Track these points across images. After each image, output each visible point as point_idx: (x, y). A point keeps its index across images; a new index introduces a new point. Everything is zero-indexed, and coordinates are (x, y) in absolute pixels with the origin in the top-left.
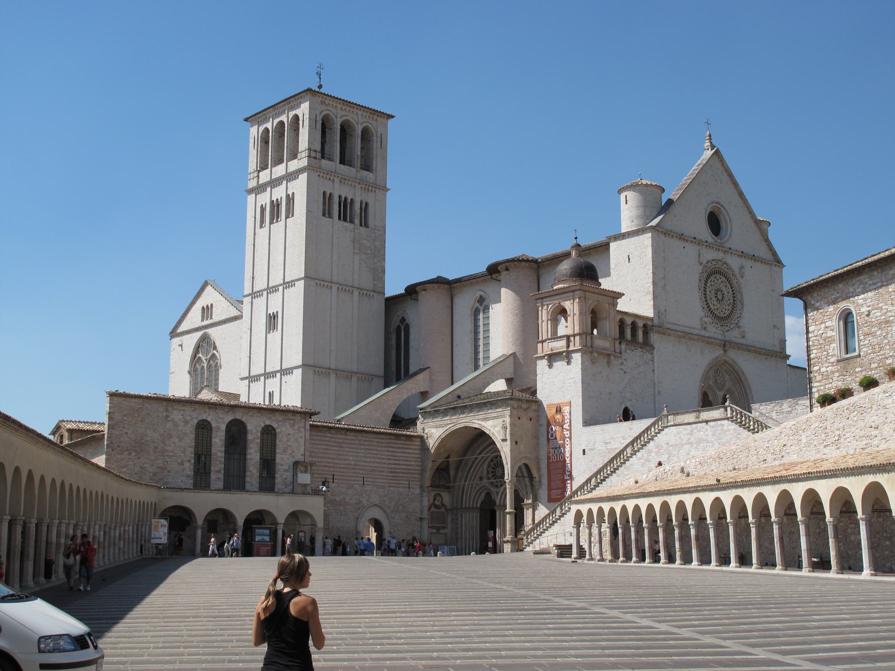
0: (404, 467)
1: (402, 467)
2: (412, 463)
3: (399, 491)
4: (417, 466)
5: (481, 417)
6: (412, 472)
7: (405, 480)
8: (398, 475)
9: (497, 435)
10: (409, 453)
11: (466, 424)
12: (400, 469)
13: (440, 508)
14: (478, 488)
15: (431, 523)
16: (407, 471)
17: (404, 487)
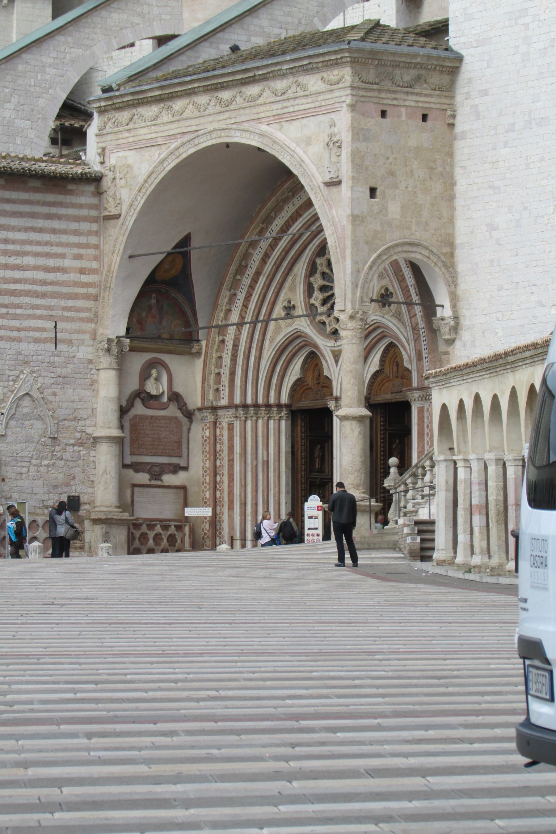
0: (40, 275)
1: (29, 274)
2: (68, 263)
3: (20, 353)
4: (82, 271)
5: (265, 111)
6: (65, 290)
7: (41, 317)
8: (16, 300)
9: (313, 168)
10: (54, 231)
12: (25, 281)
13: (164, 407)
14: (280, 338)
15: (132, 454)
16: (49, 288)
17: (37, 341)
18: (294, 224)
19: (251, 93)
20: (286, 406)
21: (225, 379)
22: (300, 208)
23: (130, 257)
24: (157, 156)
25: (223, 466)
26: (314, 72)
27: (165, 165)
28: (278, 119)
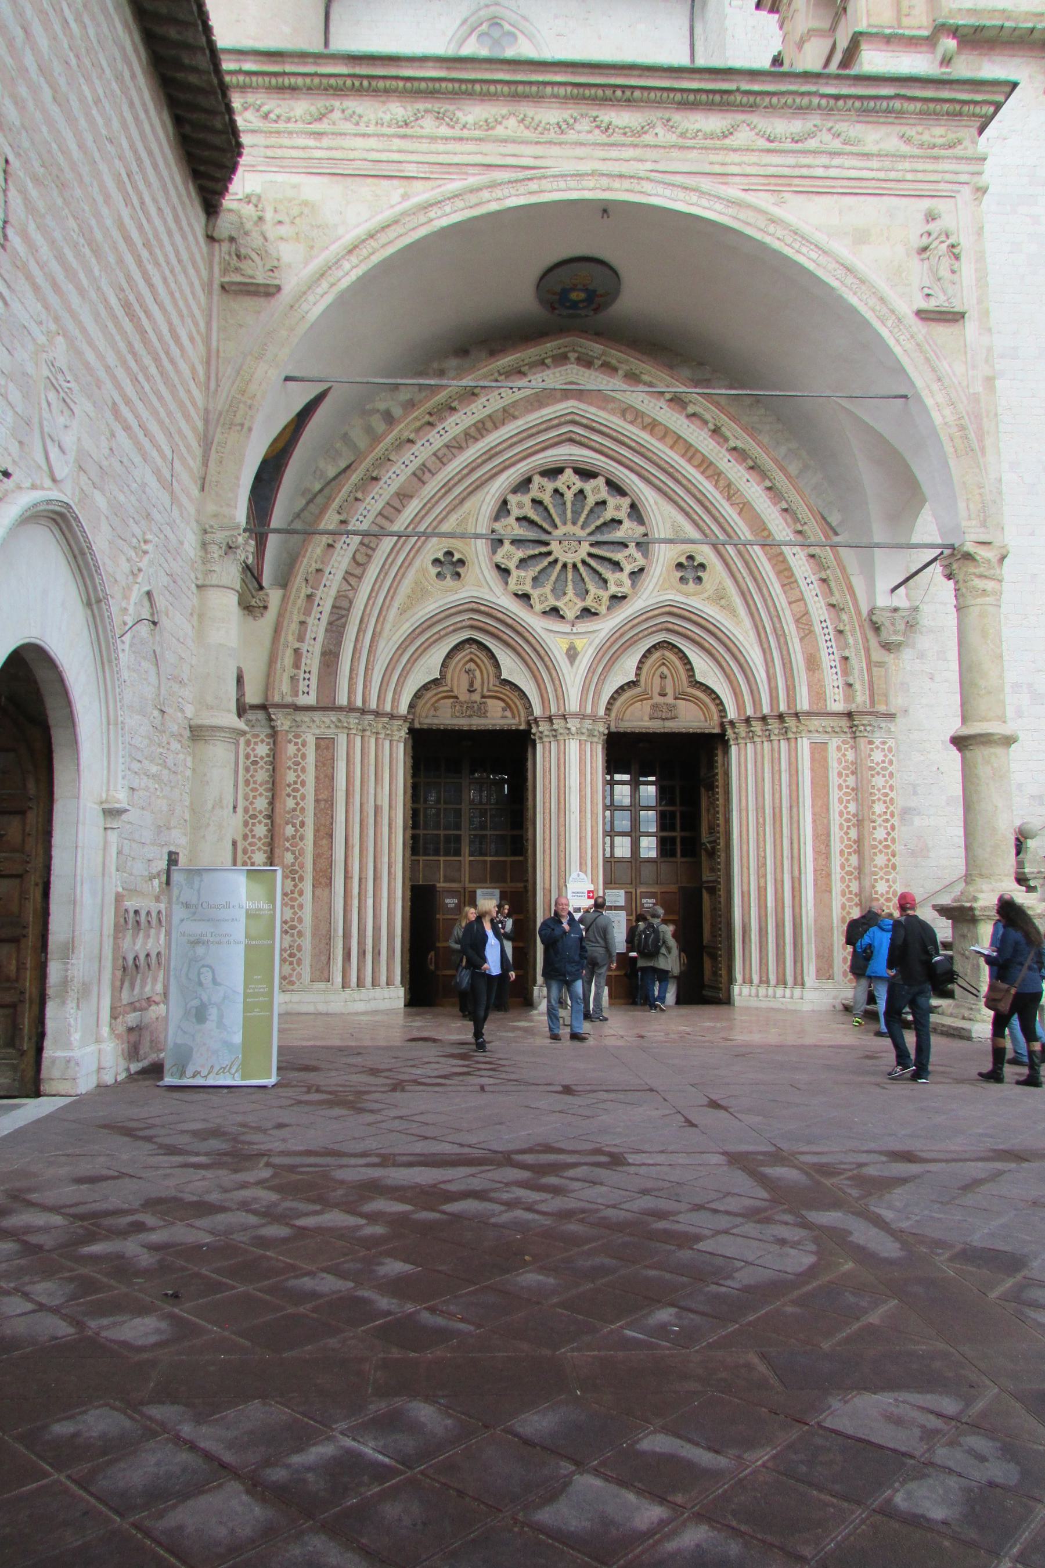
7: (161, 423)
11: (619, 193)
14: (430, 607)
18: (496, 428)
19: (697, 126)
20: (405, 719)
21: (313, 662)
22: (514, 404)
23: (287, 379)
24: (396, 197)
25: (303, 809)
26: (882, 120)
27: (432, 215)
28: (776, 185)
